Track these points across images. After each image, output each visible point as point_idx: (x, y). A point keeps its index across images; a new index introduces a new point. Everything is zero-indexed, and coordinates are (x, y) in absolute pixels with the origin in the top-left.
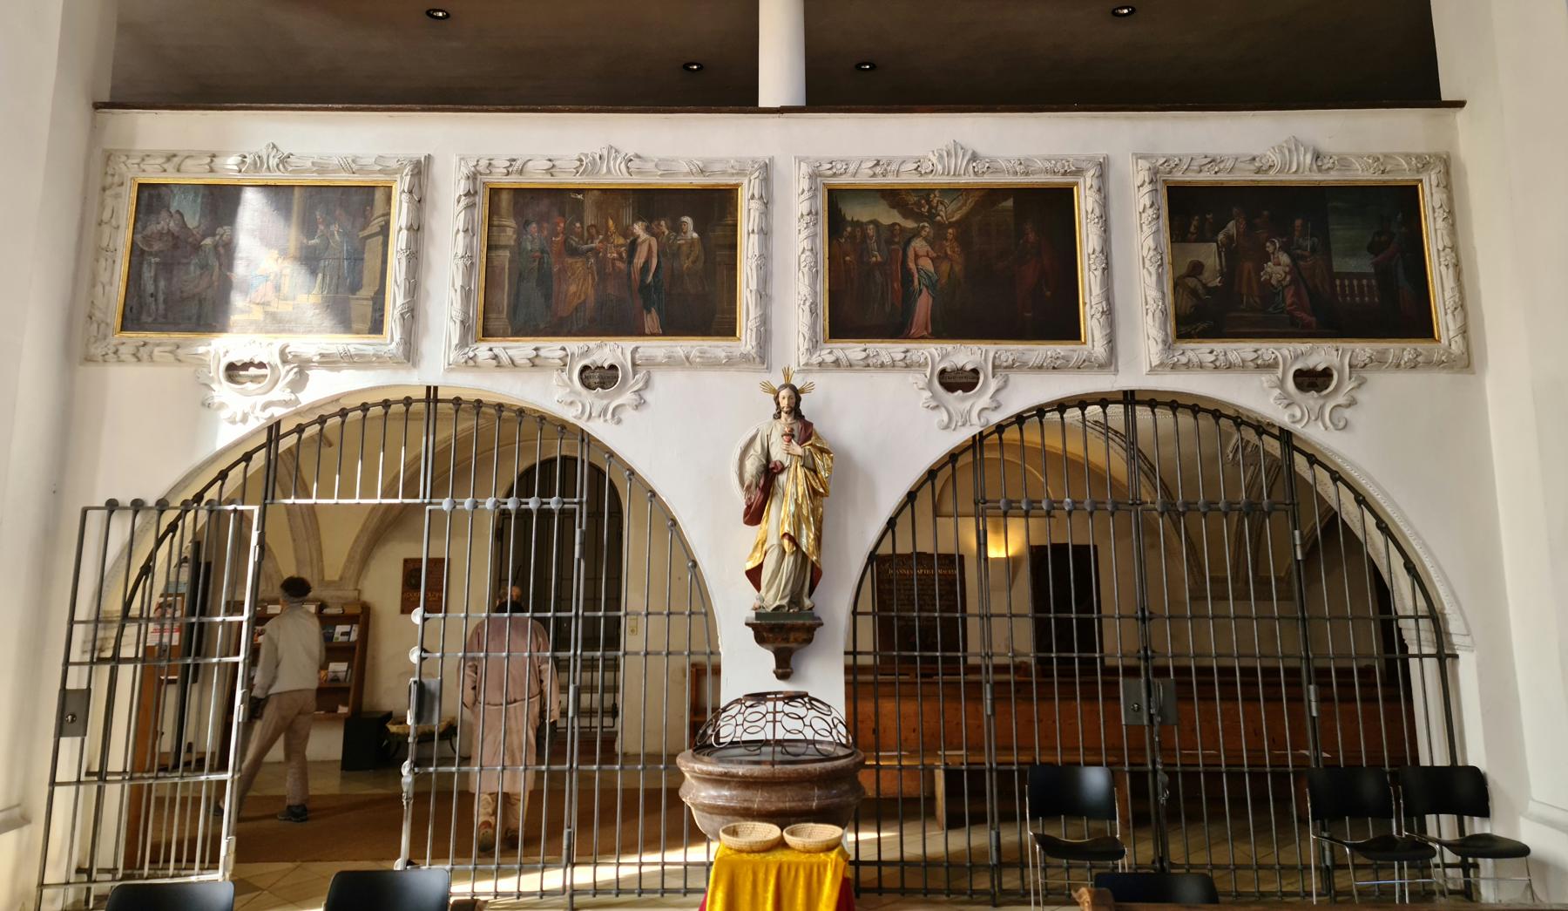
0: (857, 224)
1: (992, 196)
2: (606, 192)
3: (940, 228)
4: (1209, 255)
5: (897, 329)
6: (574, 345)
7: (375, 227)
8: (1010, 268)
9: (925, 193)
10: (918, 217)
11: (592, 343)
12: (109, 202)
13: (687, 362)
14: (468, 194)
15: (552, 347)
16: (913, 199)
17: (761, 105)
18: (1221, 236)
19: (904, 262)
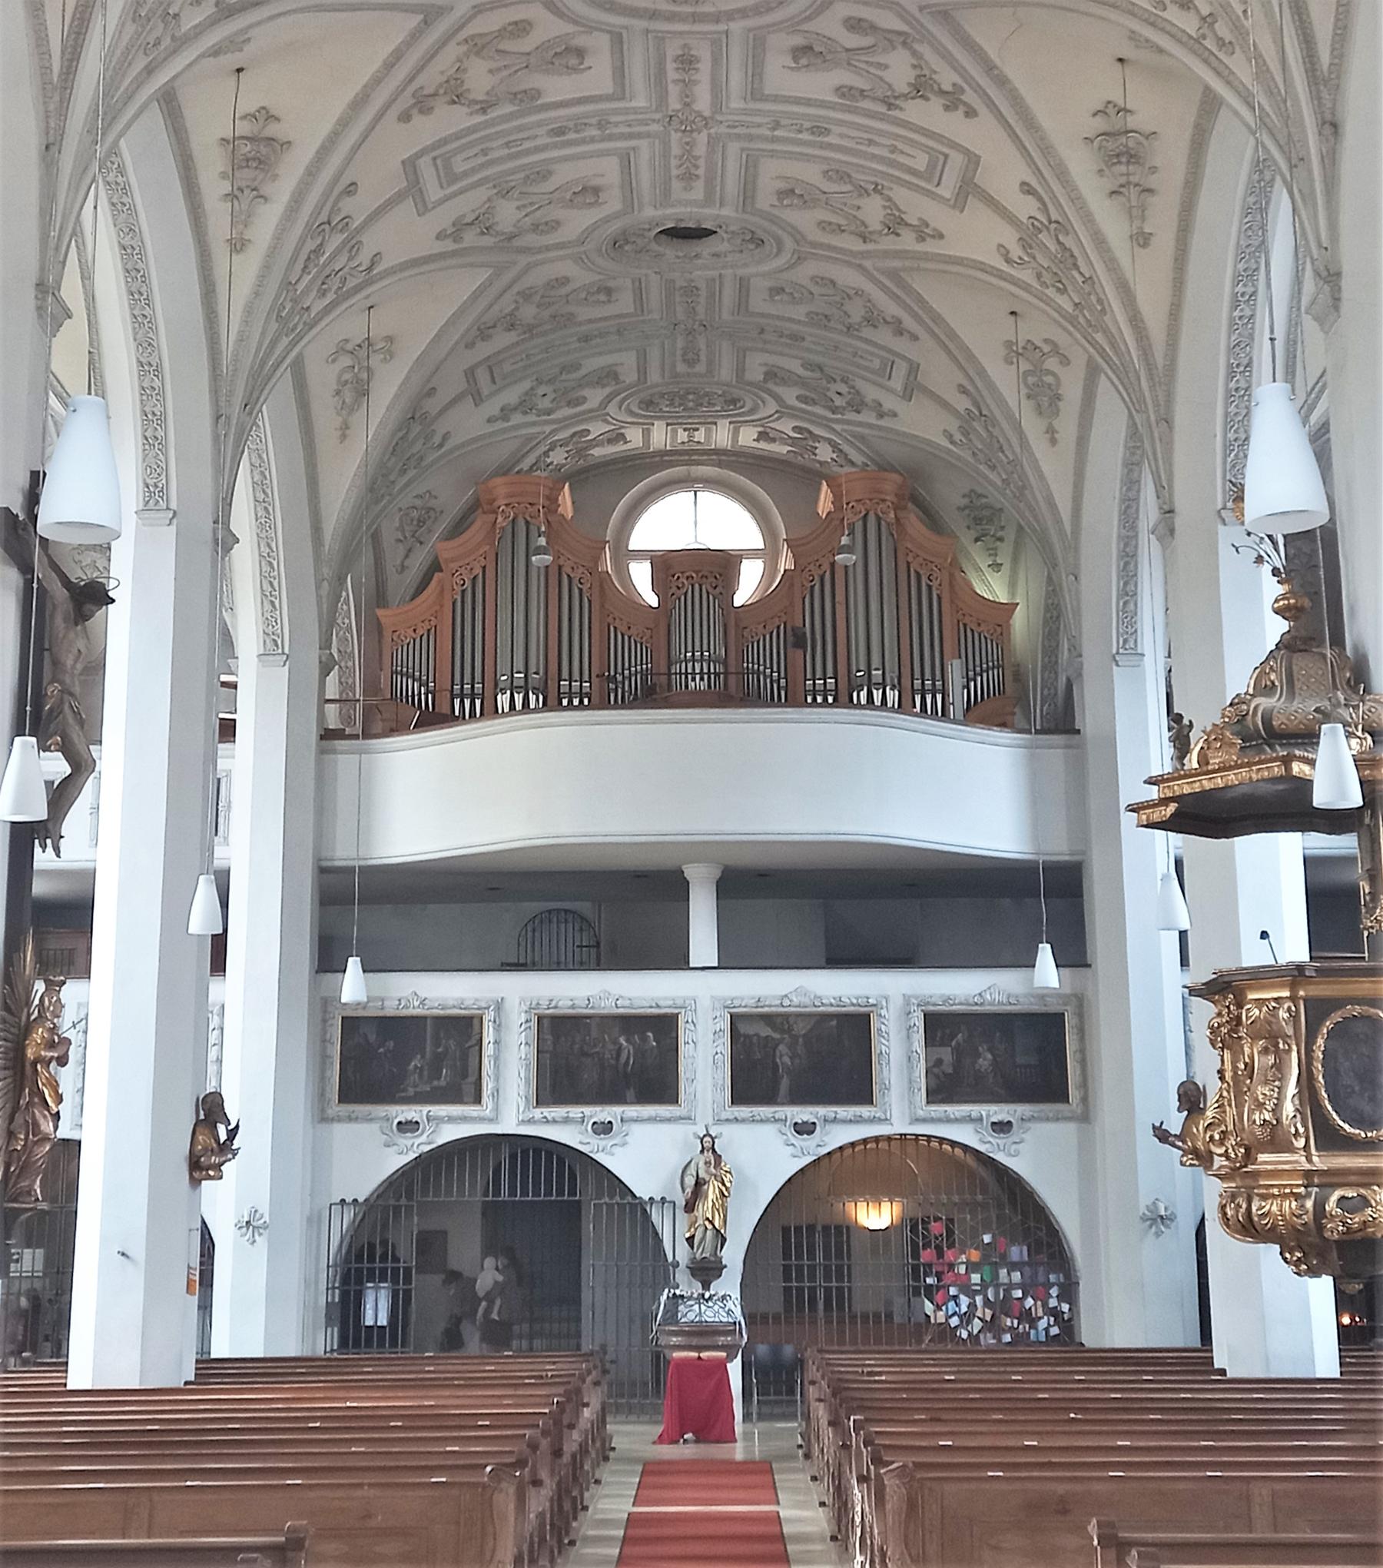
0: (747, 1036)
2: (603, 1017)
3: (795, 1038)
4: (946, 1054)
5: (768, 1098)
6: (588, 1110)
7: (473, 1041)
9: (786, 1016)
10: (782, 1031)
11: (598, 1109)
15: (575, 1111)
16: (779, 1020)
19: (774, 1056)
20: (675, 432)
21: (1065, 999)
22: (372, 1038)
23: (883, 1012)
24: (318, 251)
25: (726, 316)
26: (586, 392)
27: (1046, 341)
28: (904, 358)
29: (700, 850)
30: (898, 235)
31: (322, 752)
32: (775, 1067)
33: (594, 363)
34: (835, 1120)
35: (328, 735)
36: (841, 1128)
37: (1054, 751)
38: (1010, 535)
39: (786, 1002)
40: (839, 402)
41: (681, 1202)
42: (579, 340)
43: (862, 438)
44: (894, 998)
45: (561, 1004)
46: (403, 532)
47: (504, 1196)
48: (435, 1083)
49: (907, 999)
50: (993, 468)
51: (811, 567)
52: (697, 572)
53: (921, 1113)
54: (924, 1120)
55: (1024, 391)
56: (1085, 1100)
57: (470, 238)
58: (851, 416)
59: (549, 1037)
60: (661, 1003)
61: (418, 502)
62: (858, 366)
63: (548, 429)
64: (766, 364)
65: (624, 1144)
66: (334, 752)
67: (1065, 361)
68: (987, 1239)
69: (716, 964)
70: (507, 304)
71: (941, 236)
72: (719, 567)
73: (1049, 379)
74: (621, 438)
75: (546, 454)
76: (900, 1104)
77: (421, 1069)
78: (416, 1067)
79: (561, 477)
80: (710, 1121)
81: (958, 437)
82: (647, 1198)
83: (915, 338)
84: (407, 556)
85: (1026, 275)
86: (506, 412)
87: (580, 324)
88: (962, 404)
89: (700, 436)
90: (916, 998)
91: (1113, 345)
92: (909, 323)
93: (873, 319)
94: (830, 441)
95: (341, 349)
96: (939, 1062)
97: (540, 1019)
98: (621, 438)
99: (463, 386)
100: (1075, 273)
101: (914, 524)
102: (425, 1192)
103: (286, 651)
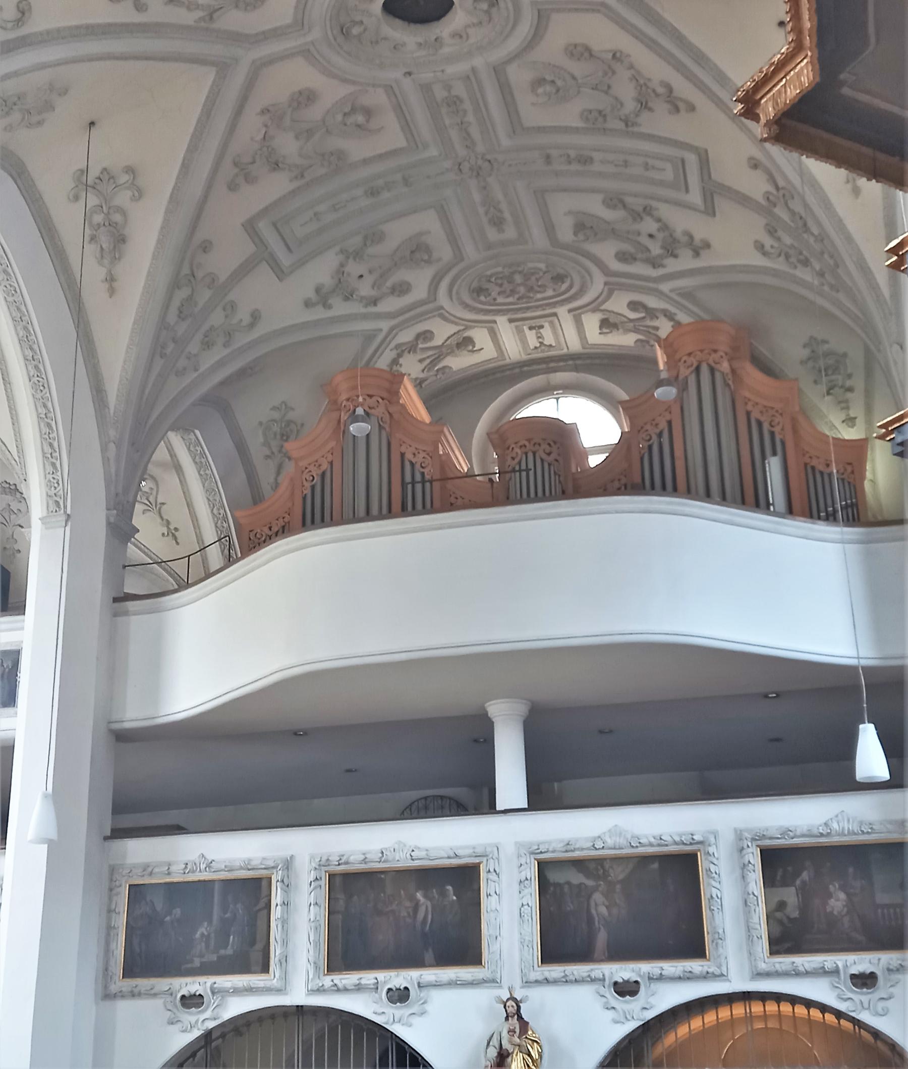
0: (557, 885)
1: (645, 860)
6: (381, 975)
7: (262, 904)
8: (659, 908)
10: (597, 878)
11: (392, 974)
12: (115, 898)
15: (368, 977)
23: (711, 850)
25: (505, 142)
32: (590, 920)
33: (399, 232)
34: (661, 978)
36: (668, 987)
39: (599, 845)
44: (725, 830)
45: (352, 859)
46: (270, 447)
48: (222, 952)
54: (768, 975)
60: (460, 852)
61: (276, 415)
63: (385, 325)
64: (570, 213)
77: (208, 937)
78: (203, 934)
80: (517, 983)
84: (278, 473)
97: (332, 877)
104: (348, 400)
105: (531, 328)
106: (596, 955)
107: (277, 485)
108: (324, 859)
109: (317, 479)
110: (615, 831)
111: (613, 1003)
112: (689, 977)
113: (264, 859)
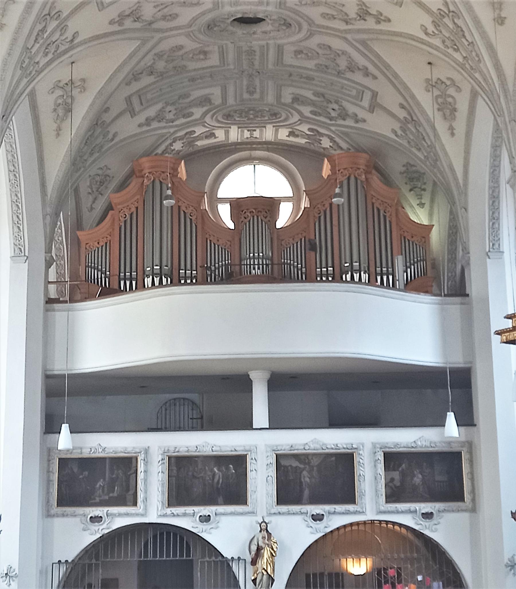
0: (285, 467)
1: (329, 455)
5: (298, 501)
6: (196, 509)
7: (133, 471)
8: (333, 480)
9: (307, 455)
10: (305, 464)
11: (202, 508)
12: (51, 465)
13: (232, 514)
14: (162, 460)
15: (190, 510)
17: (254, 427)
18: (400, 469)
19: (300, 478)
20: (243, 132)
21: (463, 444)
22: (75, 470)
23: (361, 452)
24: (43, 30)
25: (270, 66)
26: (194, 110)
27: (448, 79)
28: (369, 89)
29: (258, 363)
30: (365, 20)
31: (47, 310)
33: (197, 94)
34: (334, 513)
35: (50, 301)
36: (338, 516)
37: (454, 306)
38: (429, 187)
39: (307, 447)
40: (333, 114)
41: (249, 559)
42: (189, 80)
43: (346, 134)
44: (367, 444)
45: (181, 450)
46: (92, 189)
47: (150, 558)
49: (374, 445)
50: (419, 150)
51: (319, 206)
52: (255, 209)
53: (382, 508)
54: (384, 512)
55: (436, 106)
56: (473, 500)
57: (128, 23)
58: (340, 122)
59: (175, 468)
60: (237, 449)
61: (100, 172)
62: (344, 94)
64: (293, 94)
65: (217, 528)
66: (54, 310)
67: (459, 89)
68: (420, 578)
69: (268, 427)
70: (148, 60)
71: (389, 21)
72: (268, 206)
73: (450, 100)
74: (213, 135)
75: (171, 145)
76: (371, 503)
78: (100, 485)
79: (179, 157)
80: (265, 514)
81: (399, 132)
82: (230, 558)
83: (375, 78)
84: (94, 202)
85: (437, 42)
86: (148, 121)
87: (190, 71)
88: (402, 114)
89: (256, 134)
90: (379, 444)
91: (485, 80)
92: (372, 69)
93: (352, 67)
94: (329, 137)
95: (57, 86)
96: (392, 480)
97: (169, 458)
98: (213, 135)
99: (124, 106)
100: (464, 40)
101: (376, 180)
102: (106, 556)
103: (27, 254)
104: (149, 173)
105: (248, 131)
106: (303, 501)
107: (92, 209)
108: (166, 449)
109: (128, 217)
110: (314, 441)
111: (312, 525)
112: (347, 513)
113: (134, 448)
